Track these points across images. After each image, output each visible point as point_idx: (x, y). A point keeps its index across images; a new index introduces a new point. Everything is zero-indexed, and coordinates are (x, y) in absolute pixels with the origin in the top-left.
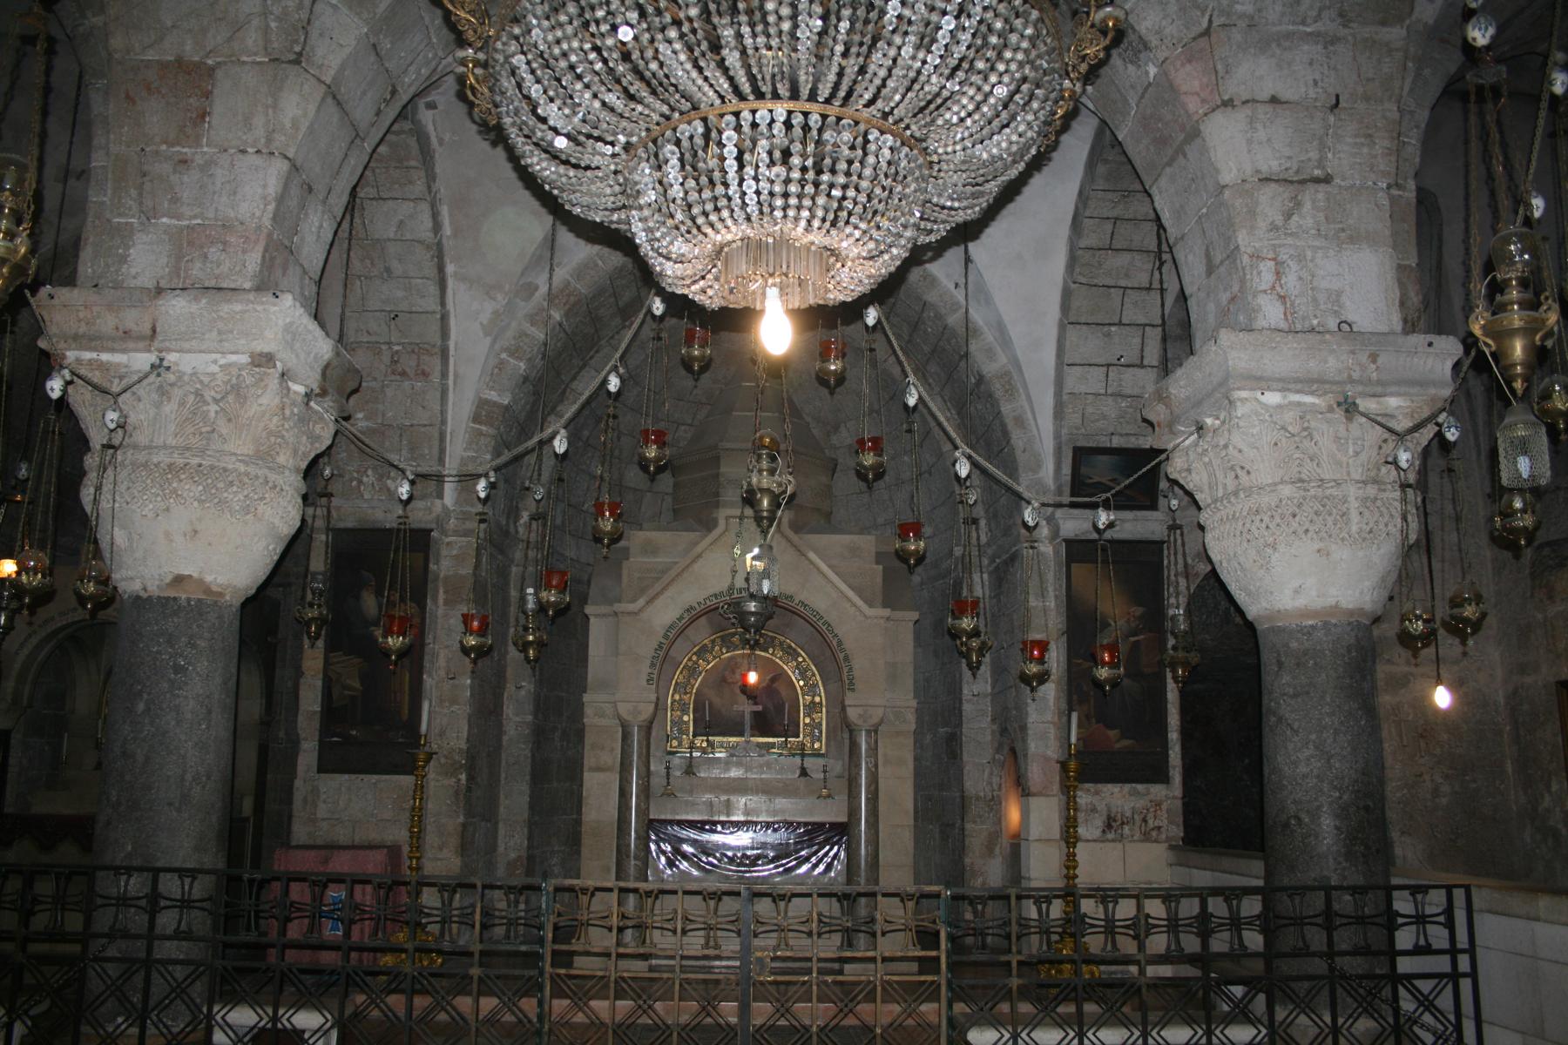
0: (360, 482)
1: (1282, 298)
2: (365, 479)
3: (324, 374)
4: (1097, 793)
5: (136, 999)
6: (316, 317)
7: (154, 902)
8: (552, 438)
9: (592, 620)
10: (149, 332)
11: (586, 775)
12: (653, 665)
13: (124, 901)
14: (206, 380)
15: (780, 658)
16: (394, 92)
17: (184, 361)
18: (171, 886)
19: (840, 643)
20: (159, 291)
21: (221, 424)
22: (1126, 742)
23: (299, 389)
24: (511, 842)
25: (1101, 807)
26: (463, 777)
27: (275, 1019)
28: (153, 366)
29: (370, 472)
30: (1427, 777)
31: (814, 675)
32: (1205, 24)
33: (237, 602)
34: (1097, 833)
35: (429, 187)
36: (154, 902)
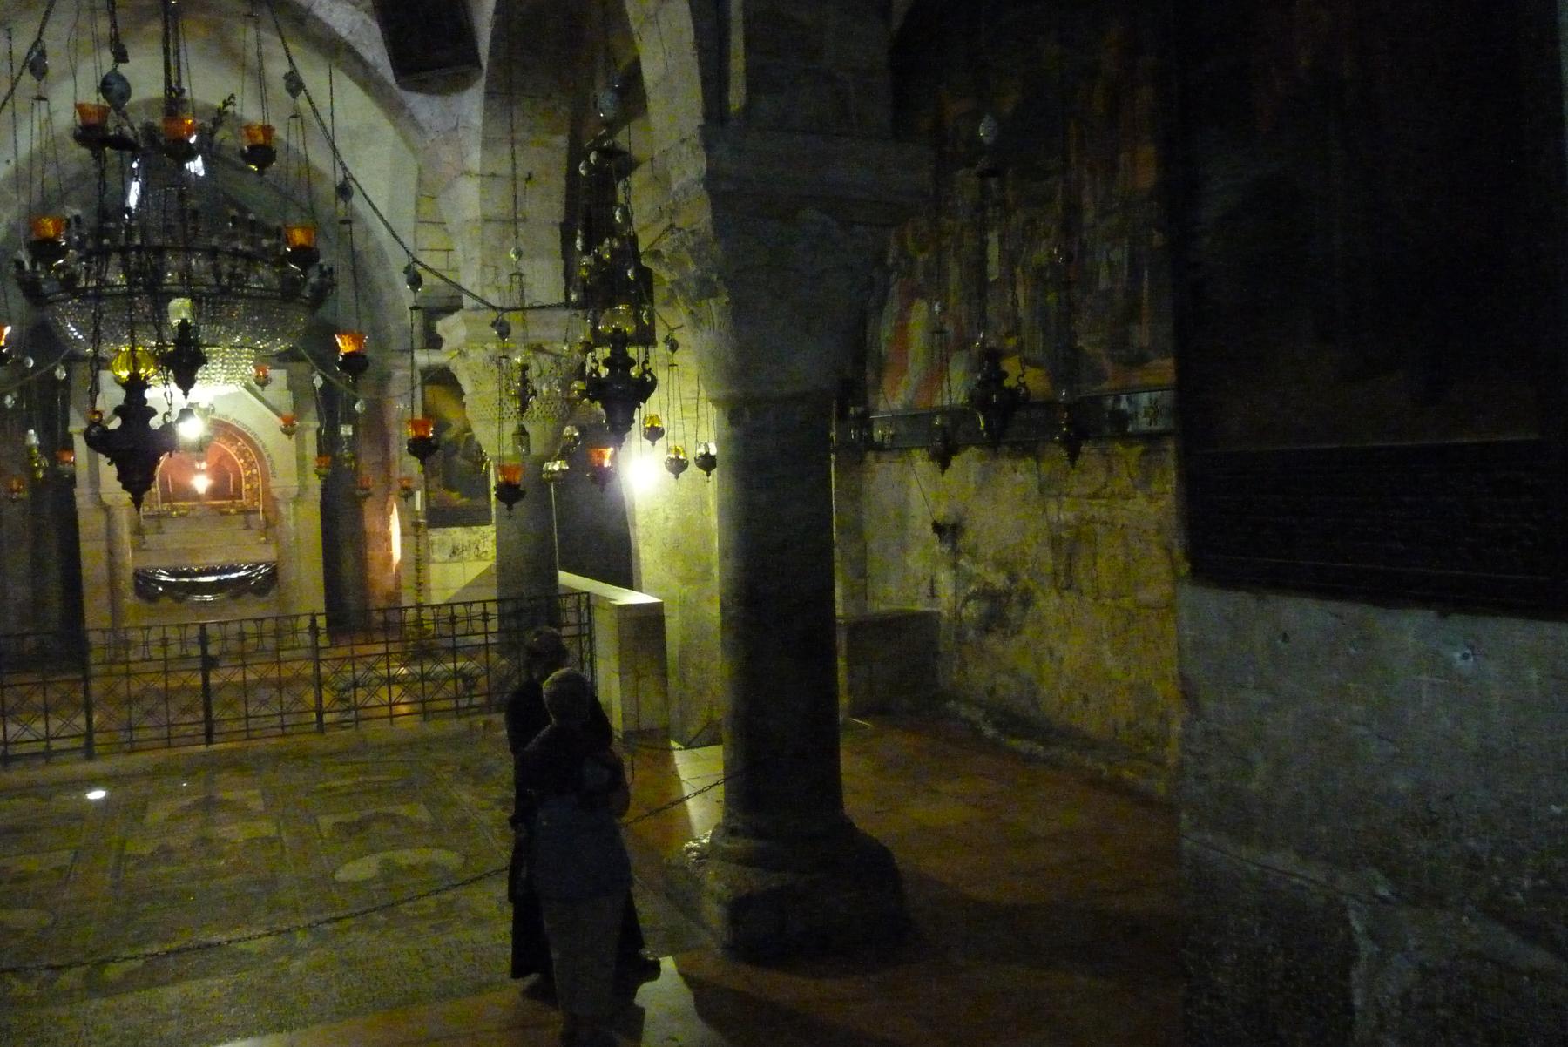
1: (499, 288)
4: (445, 533)
8: (55, 369)
11: (81, 544)
19: (264, 446)
22: (464, 500)
25: (449, 540)
30: (661, 510)
31: (251, 455)
32: (455, 123)
34: (447, 557)
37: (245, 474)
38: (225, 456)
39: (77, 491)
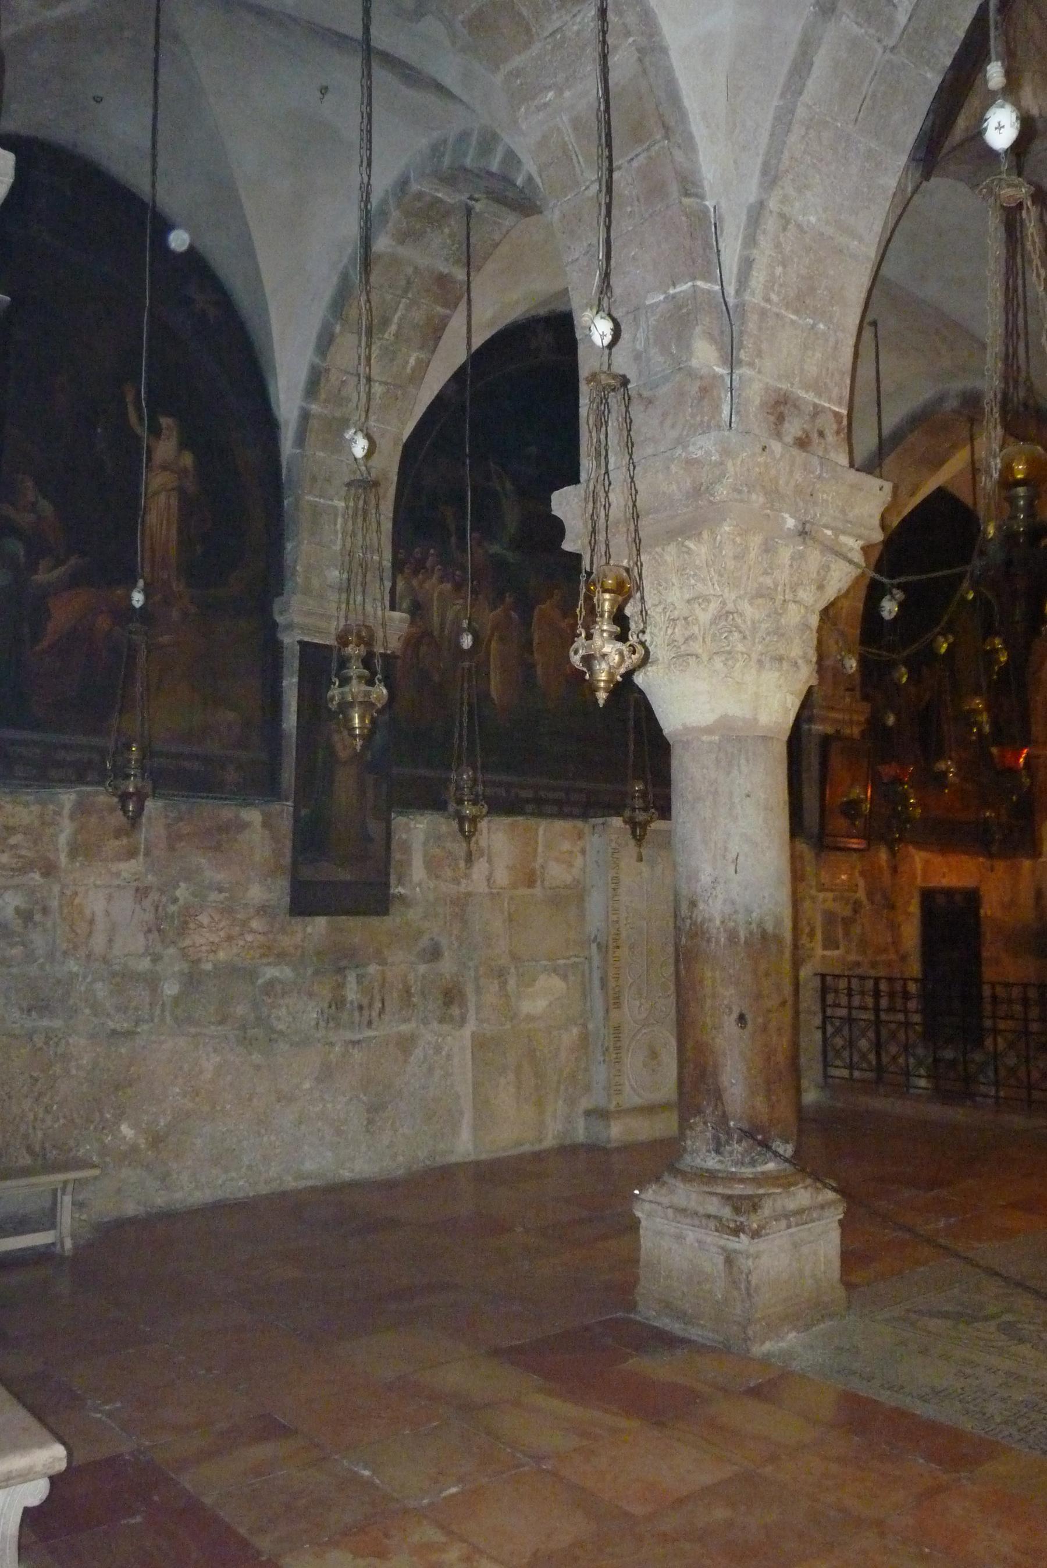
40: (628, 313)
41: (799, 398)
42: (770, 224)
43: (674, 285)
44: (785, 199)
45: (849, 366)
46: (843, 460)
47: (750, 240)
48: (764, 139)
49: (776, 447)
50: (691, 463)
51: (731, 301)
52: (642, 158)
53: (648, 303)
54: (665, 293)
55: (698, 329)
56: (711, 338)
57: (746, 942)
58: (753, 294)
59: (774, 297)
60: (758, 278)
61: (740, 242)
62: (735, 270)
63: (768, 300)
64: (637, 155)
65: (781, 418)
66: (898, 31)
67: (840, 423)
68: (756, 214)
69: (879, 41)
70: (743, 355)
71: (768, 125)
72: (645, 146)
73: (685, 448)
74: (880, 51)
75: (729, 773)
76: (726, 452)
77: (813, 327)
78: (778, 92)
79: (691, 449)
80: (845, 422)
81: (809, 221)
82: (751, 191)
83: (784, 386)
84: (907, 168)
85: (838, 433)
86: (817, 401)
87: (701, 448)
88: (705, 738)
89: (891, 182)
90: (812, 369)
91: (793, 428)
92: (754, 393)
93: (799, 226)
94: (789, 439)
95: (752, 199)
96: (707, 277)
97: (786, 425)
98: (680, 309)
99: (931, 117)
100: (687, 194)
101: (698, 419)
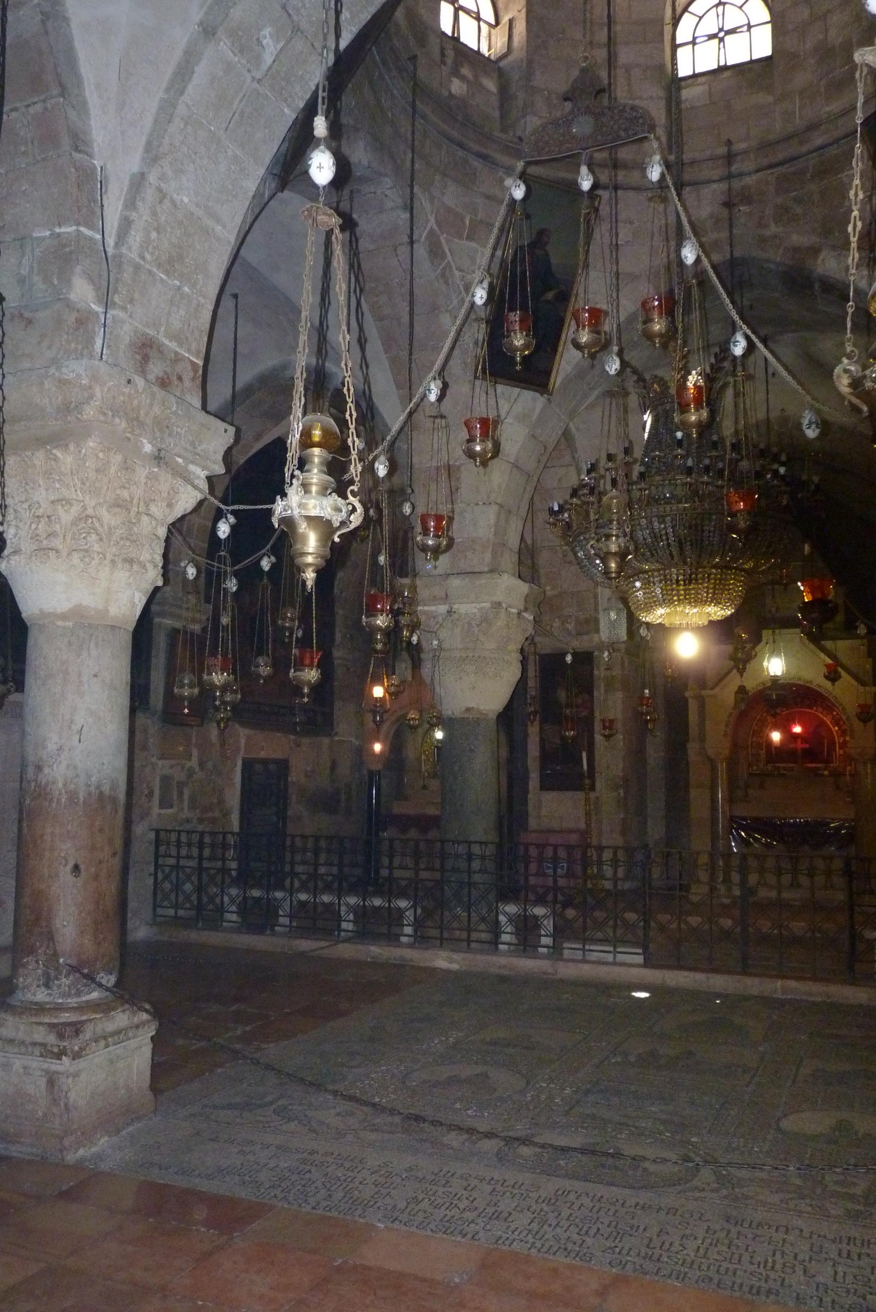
0: (552, 626)
2: (554, 625)
3: (526, 601)
5: (466, 899)
6: (520, 577)
7: (470, 857)
9: (690, 700)
10: (444, 596)
12: (727, 726)
13: (457, 856)
14: (472, 616)
15: (822, 713)
16: (545, 448)
17: (463, 608)
18: (476, 849)
20: (448, 575)
21: (482, 638)
23: (514, 611)
24: (656, 831)
26: (621, 791)
27: (525, 910)
28: (448, 612)
29: (557, 620)
33: (495, 717)
35: (573, 457)
36: (470, 857)
37: (838, 740)
38: (822, 723)
39: (689, 745)
40: (15, 240)
41: (164, 344)
42: (149, 194)
43: (60, 226)
44: (162, 177)
45: (208, 326)
46: (197, 403)
47: (131, 204)
48: (148, 122)
49: (140, 382)
50: (62, 383)
51: (110, 251)
52: (39, 107)
53: (35, 235)
54: (51, 230)
55: (78, 269)
56: (91, 280)
57: (84, 802)
58: (130, 248)
59: (148, 256)
60: (135, 238)
61: (122, 201)
62: (116, 225)
63: (143, 258)
64: (34, 103)
65: (146, 359)
66: (264, 67)
67: (196, 372)
68: (138, 182)
69: (249, 71)
70: (116, 299)
71: (153, 111)
72: (43, 97)
73: (59, 368)
74: (249, 80)
75: (79, 656)
76: (95, 378)
77: (179, 288)
78: (164, 86)
79: (64, 370)
80: (200, 372)
81: (182, 201)
82: (134, 164)
83: (151, 332)
84: (264, 180)
85: (193, 379)
86: (178, 350)
87: (73, 371)
88: (60, 623)
89: (251, 185)
90: (176, 324)
91: (156, 369)
92: (126, 333)
93: (173, 203)
94: (152, 377)
95: (135, 169)
96: (91, 227)
97: (151, 366)
98: (65, 246)
99: (286, 144)
100: (77, 149)
101: (73, 346)
